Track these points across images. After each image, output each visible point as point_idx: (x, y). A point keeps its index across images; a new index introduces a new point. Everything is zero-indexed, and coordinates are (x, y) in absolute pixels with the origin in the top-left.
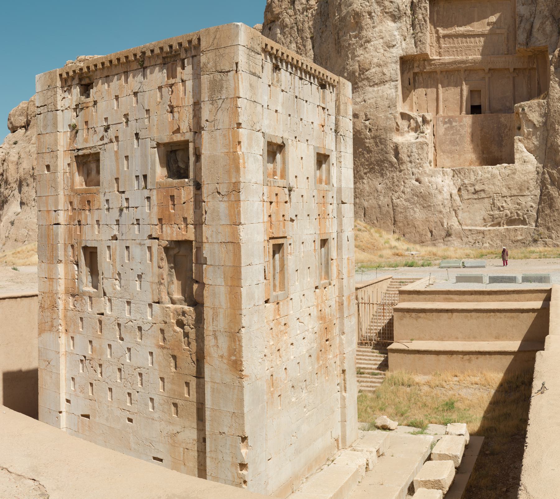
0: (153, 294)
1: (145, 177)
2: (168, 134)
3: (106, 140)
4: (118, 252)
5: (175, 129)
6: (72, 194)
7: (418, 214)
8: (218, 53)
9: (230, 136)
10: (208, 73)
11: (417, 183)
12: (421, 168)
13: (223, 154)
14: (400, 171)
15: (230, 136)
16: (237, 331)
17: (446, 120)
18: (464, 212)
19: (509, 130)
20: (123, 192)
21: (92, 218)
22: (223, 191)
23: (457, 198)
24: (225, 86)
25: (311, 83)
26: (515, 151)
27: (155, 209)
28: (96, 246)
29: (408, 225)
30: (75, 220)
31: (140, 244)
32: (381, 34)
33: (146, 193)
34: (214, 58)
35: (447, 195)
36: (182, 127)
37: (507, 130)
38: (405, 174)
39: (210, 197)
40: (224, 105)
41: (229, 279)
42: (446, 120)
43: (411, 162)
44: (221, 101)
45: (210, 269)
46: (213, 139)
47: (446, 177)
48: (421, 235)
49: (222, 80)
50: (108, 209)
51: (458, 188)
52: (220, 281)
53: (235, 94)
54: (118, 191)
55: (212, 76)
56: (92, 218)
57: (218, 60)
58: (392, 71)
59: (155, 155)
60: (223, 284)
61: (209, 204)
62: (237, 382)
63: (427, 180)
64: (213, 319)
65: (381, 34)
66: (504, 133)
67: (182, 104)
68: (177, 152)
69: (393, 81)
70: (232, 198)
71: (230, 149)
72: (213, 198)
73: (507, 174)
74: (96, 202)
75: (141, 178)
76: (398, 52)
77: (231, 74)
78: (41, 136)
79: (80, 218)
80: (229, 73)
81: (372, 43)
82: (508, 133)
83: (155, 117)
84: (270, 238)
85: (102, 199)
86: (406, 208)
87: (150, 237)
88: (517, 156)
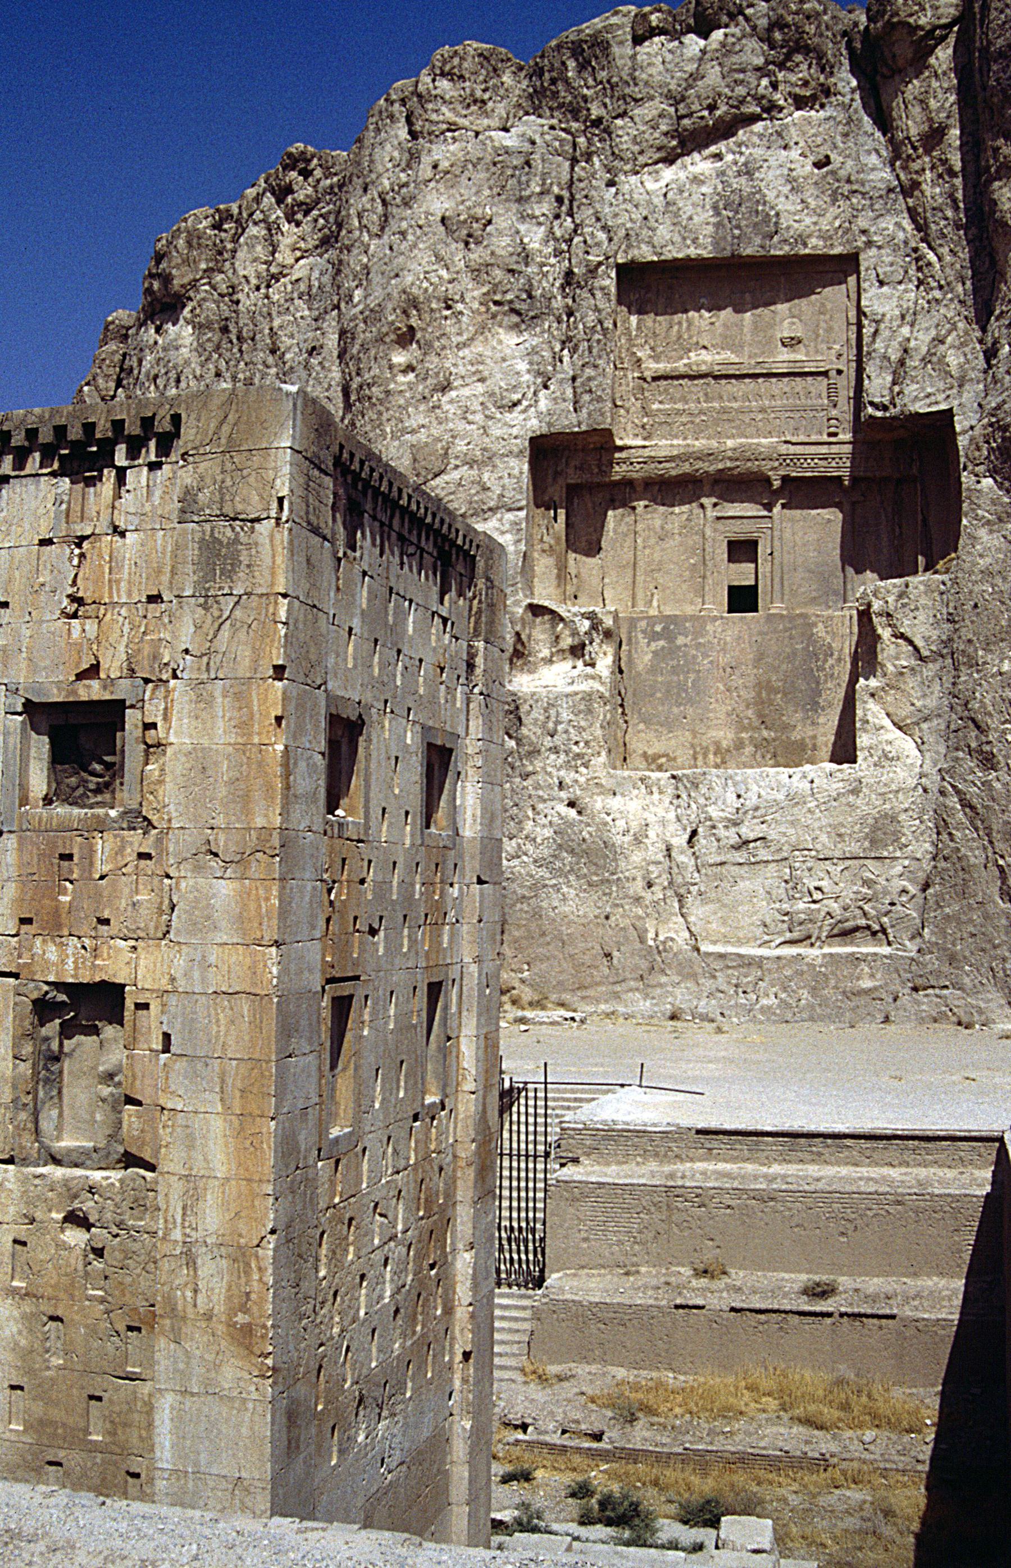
7: (571, 903)
8: (229, 466)
10: (196, 518)
11: (572, 813)
12: (582, 769)
14: (525, 776)
16: (256, 1242)
17: (658, 628)
18: (705, 902)
23: (684, 858)
25: (422, 550)
26: (858, 725)
29: (543, 934)
32: (481, 368)
34: (219, 478)
35: (655, 851)
36: (104, 665)
37: (831, 661)
38: (537, 787)
40: (238, 613)
41: (238, 1094)
42: (658, 628)
43: (555, 750)
45: (181, 1065)
46: (202, 705)
47: (656, 796)
48: (578, 967)
49: (236, 541)
51: (689, 830)
53: (273, 585)
55: (207, 527)
57: (229, 483)
58: (506, 481)
61: (183, 885)
62: (253, 1388)
63: (599, 805)
64: (184, 1208)
65: (481, 368)
67: (111, 597)
69: (510, 510)
71: (250, 735)
73: (834, 794)
76: (525, 424)
80: (257, 526)
81: (453, 394)
84: (329, 981)
86: (538, 886)
88: (863, 740)
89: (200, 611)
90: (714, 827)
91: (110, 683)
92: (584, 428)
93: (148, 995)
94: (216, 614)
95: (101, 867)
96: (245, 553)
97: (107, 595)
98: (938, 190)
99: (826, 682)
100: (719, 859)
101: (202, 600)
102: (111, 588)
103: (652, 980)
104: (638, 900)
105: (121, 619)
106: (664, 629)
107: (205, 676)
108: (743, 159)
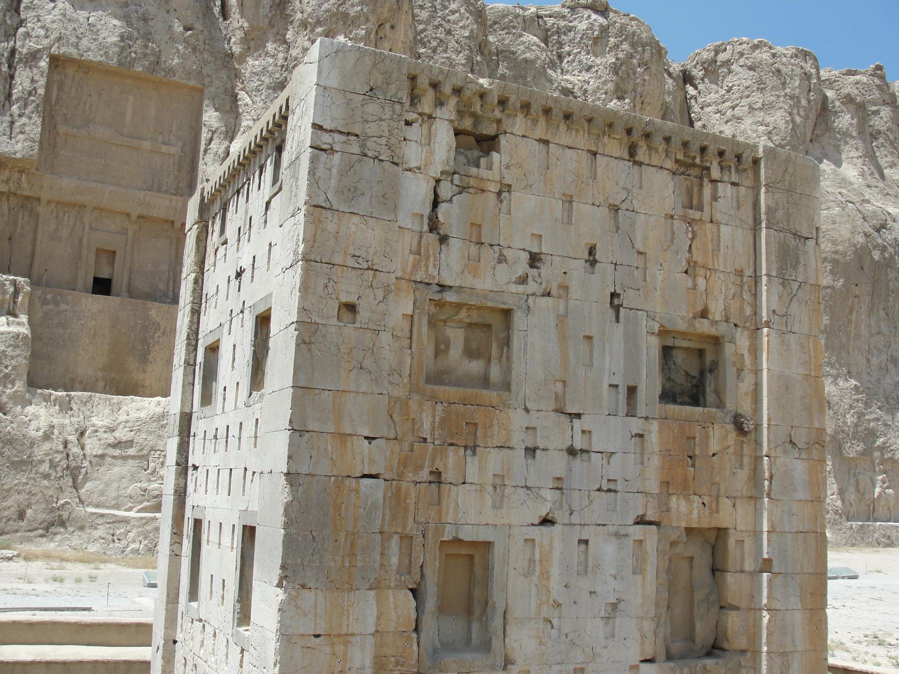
0: (642, 643)
1: (632, 391)
2: (684, 313)
3: (532, 287)
4: (556, 553)
5: (699, 308)
6: (416, 397)
9: (811, 347)
13: (800, 378)
15: (811, 347)
19: (163, 334)
20: (578, 416)
21: (482, 469)
22: (801, 442)
24: (802, 262)
27: (655, 462)
28: (490, 539)
30: (419, 467)
31: (617, 535)
33: (636, 425)
37: (159, 334)
39: (779, 449)
40: (800, 294)
44: (796, 285)
49: (797, 248)
50: (531, 451)
52: (794, 602)
54: (560, 411)
55: (782, 235)
56: (482, 469)
59: (651, 348)
60: (799, 607)
61: (778, 461)
66: (153, 337)
67: (713, 265)
68: (674, 352)
70: (815, 454)
71: (810, 371)
72: (785, 452)
74: (496, 427)
75: (623, 390)
77: (811, 243)
78: (329, 214)
79: (439, 465)
82: (161, 340)
83: (658, 272)
85: (517, 419)
87: (641, 521)
89: (780, 286)
90: (96, 431)
91: (714, 323)
92: (18, 156)
93: (743, 534)
94: (789, 291)
95: (714, 447)
96: (802, 256)
97: (711, 263)
98: (257, 62)
99: (154, 345)
100: (100, 452)
101: (781, 281)
102: (713, 259)
103: (52, 529)
104: (46, 476)
105: (720, 281)
106: (52, 298)
107: (785, 329)
108: (141, 11)
